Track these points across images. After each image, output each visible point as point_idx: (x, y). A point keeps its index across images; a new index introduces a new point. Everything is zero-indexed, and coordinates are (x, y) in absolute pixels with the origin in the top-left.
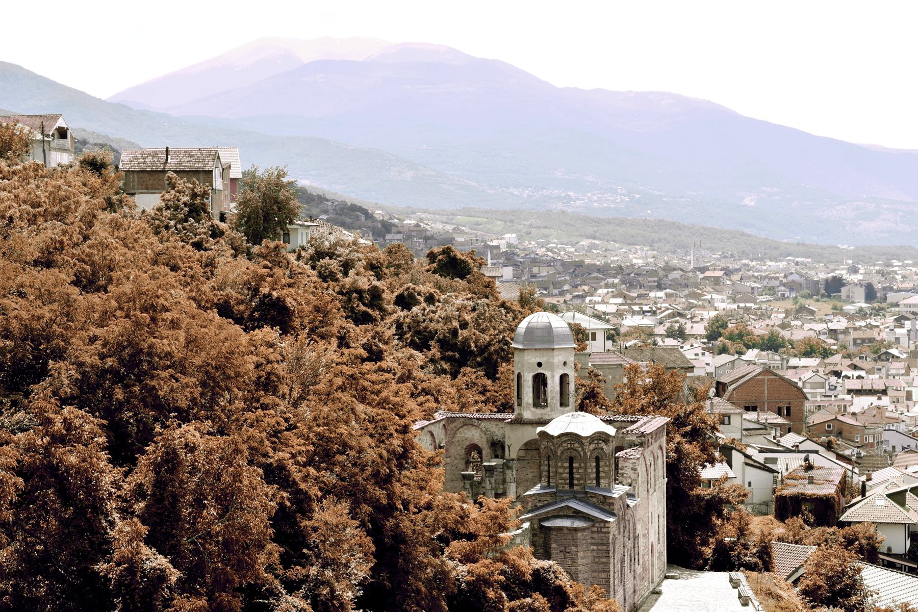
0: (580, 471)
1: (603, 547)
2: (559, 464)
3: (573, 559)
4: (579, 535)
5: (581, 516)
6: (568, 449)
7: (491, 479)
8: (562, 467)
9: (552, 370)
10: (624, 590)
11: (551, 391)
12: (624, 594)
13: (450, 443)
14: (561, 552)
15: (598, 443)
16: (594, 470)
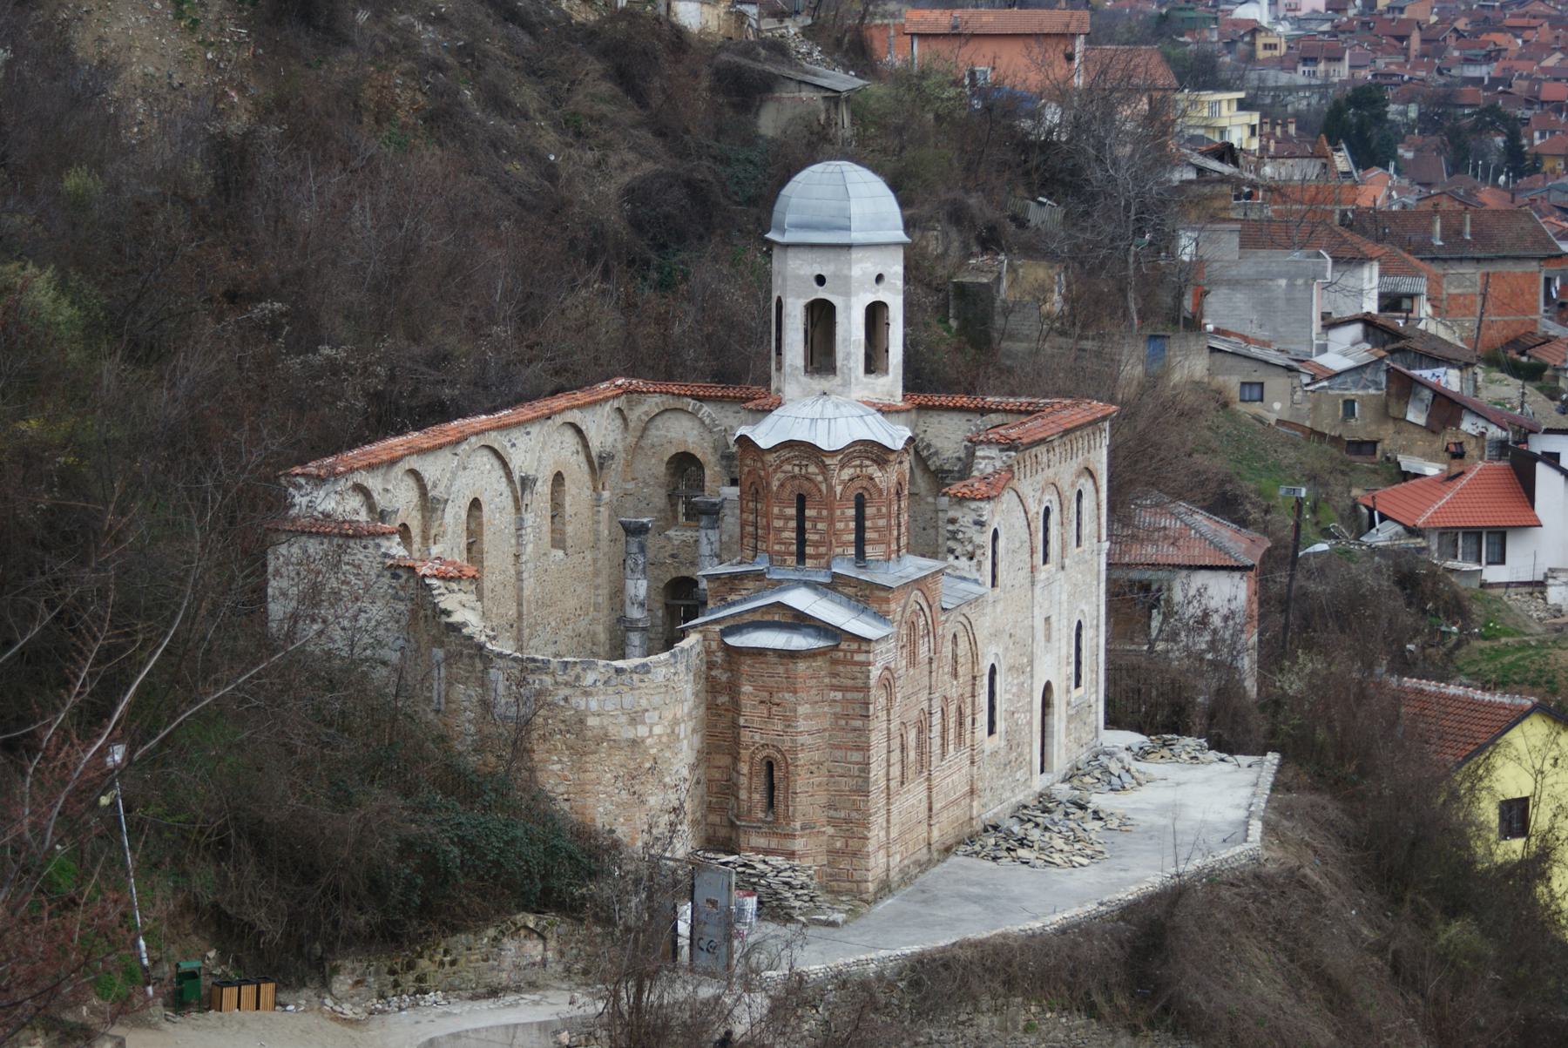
0: (820, 526)
2: (776, 510)
4: (802, 666)
5: (809, 626)
6: (794, 477)
7: (710, 532)
8: (781, 516)
9: (847, 294)
10: (930, 789)
11: (845, 340)
12: (929, 797)
13: (635, 450)
14: (762, 702)
15: (861, 466)
16: (852, 525)
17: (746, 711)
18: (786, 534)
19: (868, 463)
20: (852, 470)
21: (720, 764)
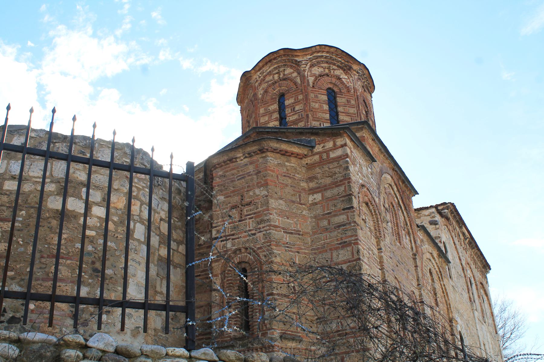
0: (297, 108)
1: (335, 191)
3: (257, 214)
19: (334, 67)
20: (321, 70)
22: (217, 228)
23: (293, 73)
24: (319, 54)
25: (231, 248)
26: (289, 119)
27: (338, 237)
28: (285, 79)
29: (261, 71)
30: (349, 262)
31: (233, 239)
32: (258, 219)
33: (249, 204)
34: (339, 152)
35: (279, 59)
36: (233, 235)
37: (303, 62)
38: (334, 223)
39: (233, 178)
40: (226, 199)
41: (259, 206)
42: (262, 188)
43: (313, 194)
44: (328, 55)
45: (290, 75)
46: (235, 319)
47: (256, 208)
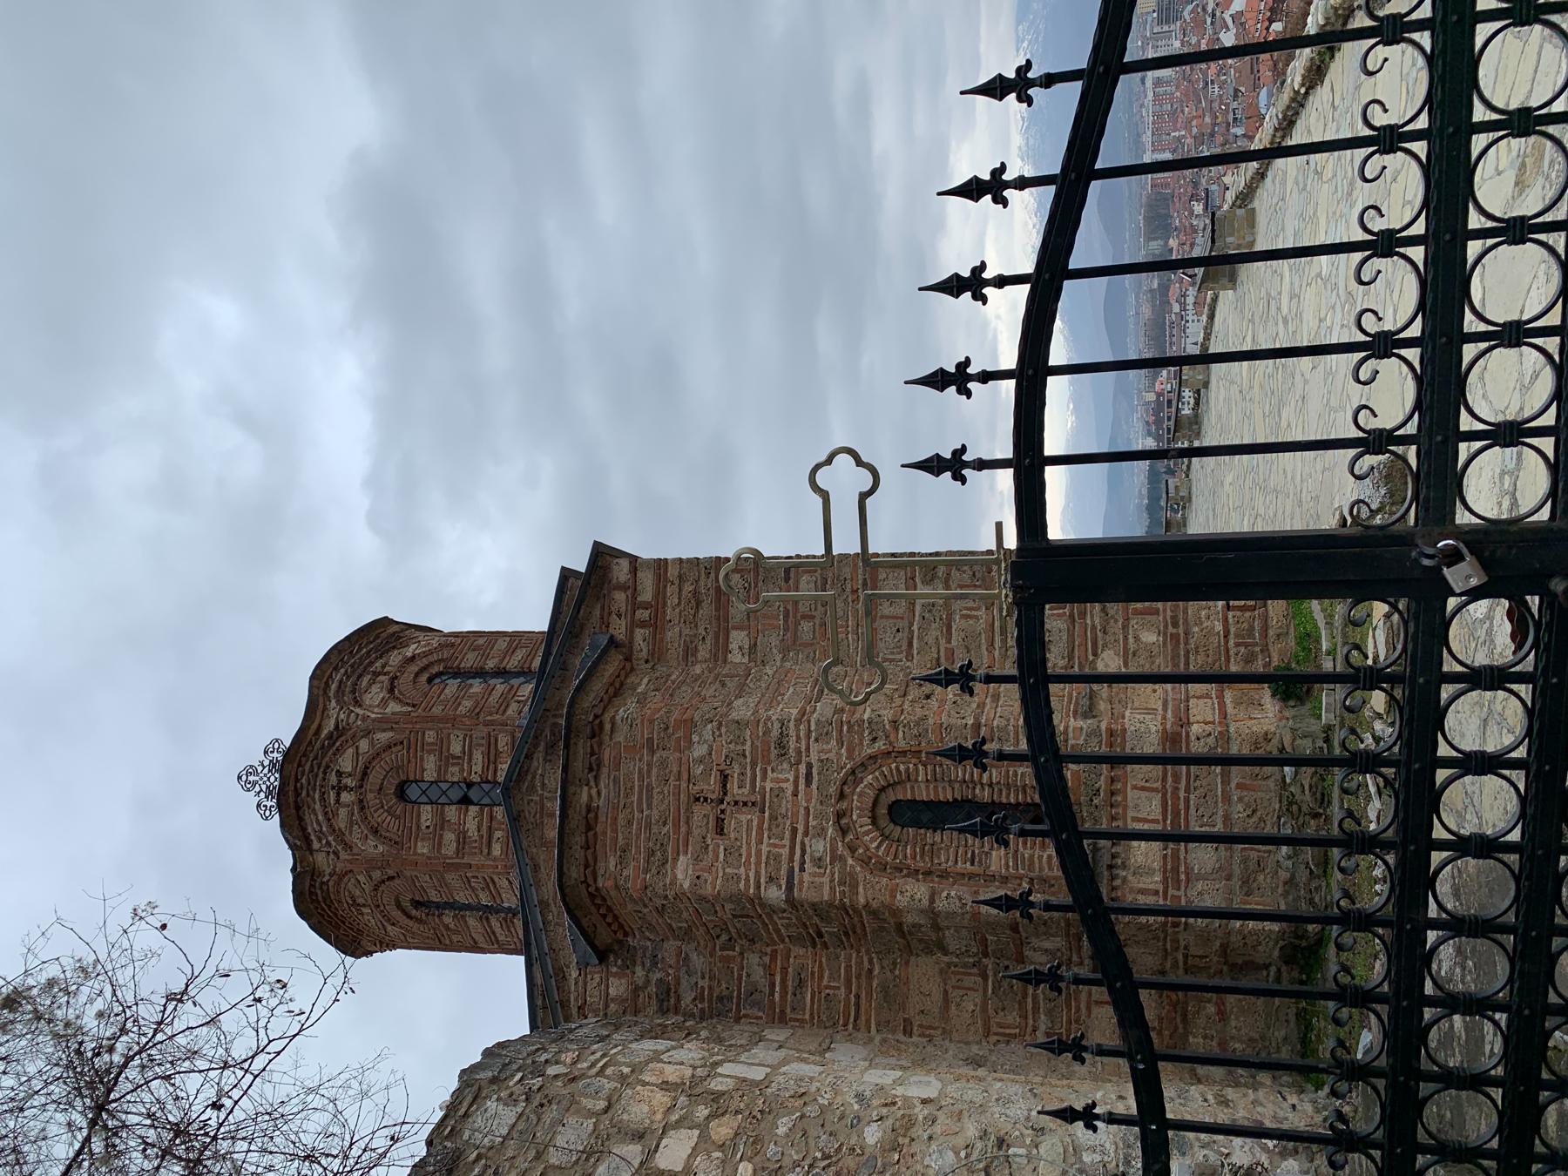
14: (720, 830)
17: (747, 877)
18: (471, 826)
19: (378, 664)
21: (937, 996)
22: (762, 880)
23: (357, 747)
24: (334, 686)
25: (828, 839)
26: (476, 773)
27: (850, 600)
28: (365, 774)
29: (313, 837)
30: (913, 578)
31: (806, 834)
32: (774, 752)
33: (725, 778)
34: (647, 581)
35: (303, 781)
36: (794, 831)
37: (342, 716)
38: (813, 606)
39: (638, 824)
40: (690, 848)
41: (739, 747)
42: (695, 738)
43: (727, 651)
44: (342, 671)
45: (360, 758)
46: (1020, 844)
47: (742, 759)
